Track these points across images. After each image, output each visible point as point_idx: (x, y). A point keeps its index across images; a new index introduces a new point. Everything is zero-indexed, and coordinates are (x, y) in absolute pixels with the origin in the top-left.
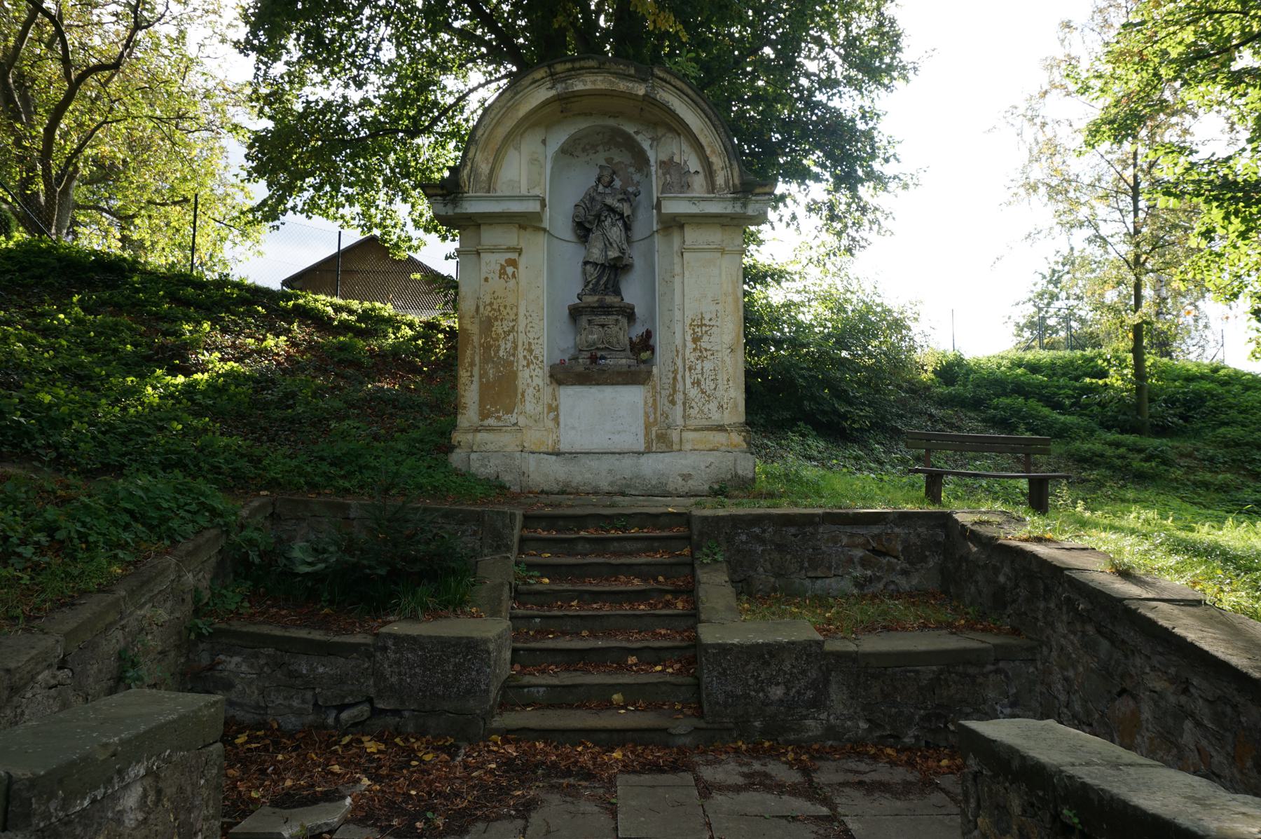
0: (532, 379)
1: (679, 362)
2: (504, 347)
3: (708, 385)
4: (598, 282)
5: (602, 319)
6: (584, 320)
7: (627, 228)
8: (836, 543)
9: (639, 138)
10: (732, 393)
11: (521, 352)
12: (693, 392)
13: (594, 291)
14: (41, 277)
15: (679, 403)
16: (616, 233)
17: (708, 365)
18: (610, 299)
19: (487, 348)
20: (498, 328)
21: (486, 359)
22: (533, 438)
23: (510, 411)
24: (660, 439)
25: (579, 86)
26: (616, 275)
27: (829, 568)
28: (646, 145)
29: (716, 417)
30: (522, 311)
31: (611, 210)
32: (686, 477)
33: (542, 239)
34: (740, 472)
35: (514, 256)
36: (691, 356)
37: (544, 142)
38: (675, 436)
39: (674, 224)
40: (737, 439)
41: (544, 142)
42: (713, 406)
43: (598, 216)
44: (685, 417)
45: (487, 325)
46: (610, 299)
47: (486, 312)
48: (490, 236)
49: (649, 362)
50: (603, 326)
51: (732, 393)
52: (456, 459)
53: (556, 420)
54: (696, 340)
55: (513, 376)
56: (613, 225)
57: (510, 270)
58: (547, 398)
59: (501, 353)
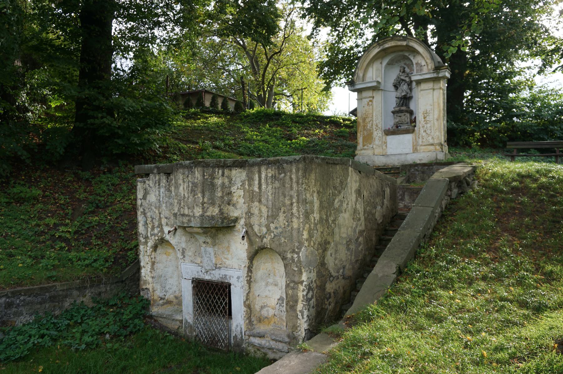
0: (378, 134)
1: (420, 125)
2: (369, 125)
3: (428, 132)
5: (400, 114)
9: (410, 57)
10: (437, 133)
11: (374, 127)
12: (424, 134)
13: (398, 106)
14: (260, 119)
15: (420, 138)
16: (405, 87)
17: (428, 125)
18: (404, 108)
19: (364, 126)
20: (367, 120)
21: (364, 130)
22: (377, 151)
23: (371, 144)
24: (415, 150)
25: (387, 46)
28: (412, 58)
29: (431, 141)
30: (374, 114)
31: (403, 80)
32: (420, 160)
33: (380, 92)
34: (439, 158)
35: (371, 99)
36: (423, 122)
37: (381, 63)
38: (418, 148)
39: (419, 82)
40: (438, 148)
41: (381, 63)
42: (430, 138)
43: (399, 82)
44: (422, 142)
45: (364, 120)
46: (404, 108)
47: (364, 116)
48: (365, 94)
49: (415, 126)
51: (437, 133)
52: (356, 158)
53: (386, 146)
54: (425, 118)
55: (372, 133)
57: (370, 103)
58: (384, 140)
59: (368, 127)
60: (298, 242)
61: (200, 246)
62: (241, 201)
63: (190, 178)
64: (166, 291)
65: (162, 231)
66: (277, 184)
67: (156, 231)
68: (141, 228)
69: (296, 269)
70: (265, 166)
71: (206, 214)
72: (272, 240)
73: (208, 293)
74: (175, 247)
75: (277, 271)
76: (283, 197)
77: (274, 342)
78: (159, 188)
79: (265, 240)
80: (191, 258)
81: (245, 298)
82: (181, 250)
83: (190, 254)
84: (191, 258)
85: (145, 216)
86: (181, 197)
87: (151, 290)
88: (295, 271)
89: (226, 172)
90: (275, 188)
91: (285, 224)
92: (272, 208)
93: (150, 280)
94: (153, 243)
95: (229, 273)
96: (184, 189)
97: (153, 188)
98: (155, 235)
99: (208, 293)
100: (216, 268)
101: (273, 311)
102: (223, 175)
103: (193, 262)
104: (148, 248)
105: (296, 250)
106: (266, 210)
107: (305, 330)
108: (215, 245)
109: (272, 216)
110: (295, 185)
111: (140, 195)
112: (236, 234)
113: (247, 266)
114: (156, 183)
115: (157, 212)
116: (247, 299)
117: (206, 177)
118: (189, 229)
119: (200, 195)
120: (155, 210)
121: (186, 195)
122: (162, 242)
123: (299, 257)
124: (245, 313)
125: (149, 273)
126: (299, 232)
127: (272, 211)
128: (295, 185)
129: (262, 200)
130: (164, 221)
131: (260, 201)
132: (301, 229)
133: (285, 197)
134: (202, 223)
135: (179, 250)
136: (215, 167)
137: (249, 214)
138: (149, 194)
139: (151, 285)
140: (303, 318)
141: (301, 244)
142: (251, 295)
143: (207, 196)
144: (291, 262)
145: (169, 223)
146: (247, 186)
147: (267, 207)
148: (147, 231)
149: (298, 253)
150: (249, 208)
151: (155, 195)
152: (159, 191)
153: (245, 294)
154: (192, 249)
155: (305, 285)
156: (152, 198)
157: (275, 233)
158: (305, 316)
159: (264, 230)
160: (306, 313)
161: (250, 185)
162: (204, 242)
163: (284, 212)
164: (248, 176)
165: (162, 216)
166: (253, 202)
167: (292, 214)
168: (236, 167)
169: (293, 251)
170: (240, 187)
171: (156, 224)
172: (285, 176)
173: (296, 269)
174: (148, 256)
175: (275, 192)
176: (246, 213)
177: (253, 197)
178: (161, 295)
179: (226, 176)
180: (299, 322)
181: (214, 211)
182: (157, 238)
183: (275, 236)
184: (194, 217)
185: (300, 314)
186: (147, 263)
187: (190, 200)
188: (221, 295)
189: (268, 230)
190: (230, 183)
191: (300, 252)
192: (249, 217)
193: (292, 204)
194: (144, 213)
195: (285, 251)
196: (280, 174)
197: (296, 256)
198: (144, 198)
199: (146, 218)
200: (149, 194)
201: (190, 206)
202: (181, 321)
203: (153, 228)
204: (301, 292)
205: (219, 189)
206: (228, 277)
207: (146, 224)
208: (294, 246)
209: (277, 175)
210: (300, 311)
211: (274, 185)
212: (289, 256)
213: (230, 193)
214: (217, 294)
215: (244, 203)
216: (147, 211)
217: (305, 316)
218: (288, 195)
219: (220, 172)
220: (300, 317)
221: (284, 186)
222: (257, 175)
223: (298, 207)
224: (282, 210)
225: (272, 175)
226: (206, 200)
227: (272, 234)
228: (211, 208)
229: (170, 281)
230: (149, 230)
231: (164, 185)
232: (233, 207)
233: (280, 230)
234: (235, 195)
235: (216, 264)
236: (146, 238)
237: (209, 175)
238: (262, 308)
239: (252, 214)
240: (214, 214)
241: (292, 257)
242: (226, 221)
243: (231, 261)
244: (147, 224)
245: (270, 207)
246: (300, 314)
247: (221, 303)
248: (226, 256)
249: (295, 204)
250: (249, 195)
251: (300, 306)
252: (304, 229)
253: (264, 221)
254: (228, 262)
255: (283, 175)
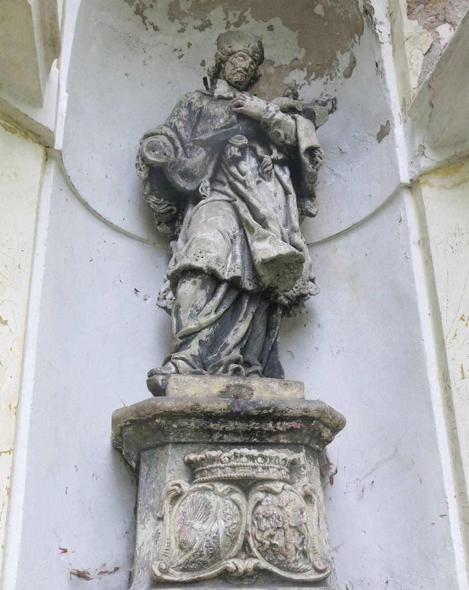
4: (214, 344)
5: (242, 460)
6: (169, 469)
7: (304, 188)
13: (204, 365)
16: (271, 195)
26: (269, 327)
50: (246, 485)
56: (264, 174)
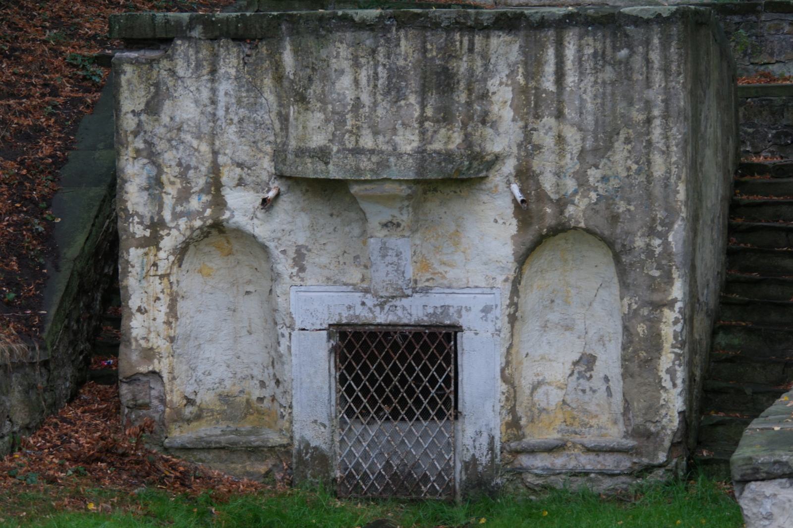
8: (778, 30)
27: (772, 55)
60: (666, 210)
61: (364, 235)
62: (508, 114)
63: (381, 58)
64: (198, 382)
65: (219, 203)
66: (609, 74)
67: (195, 204)
68: (135, 197)
69: (656, 273)
70: (577, 30)
71: (430, 147)
72: (592, 208)
73: (387, 359)
74: (271, 245)
75: (573, 292)
76: (624, 104)
77: (592, 456)
78: (213, 81)
79: (570, 210)
80: (326, 272)
81: (504, 360)
82: (292, 253)
83: (324, 260)
84: (326, 272)
85: (153, 163)
86: (344, 106)
87: (165, 375)
88: (653, 278)
89: (478, 39)
90: (604, 83)
91: (629, 169)
92: (595, 132)
93: (160, 344)
94: (181, 239)
95: (454, 300)
96: (356, 82)
97: (188, 82)
98: (190, 215)
99: (387, 359)
100: (415, 291)
101: (561, 393)
102: (471, 50)
103: (335, 282)
104: (162, 254)
105: (659, 228)
106: (578, 136)
107: (680, 413)
108: (417, 230)
109: (595, 150)
110: (657, 78)
111: (131, 101)
112: (485, 198)
113: (511, 278)
114: (198, 66)
115: (204, 148)
116: (508, 363)
117: (429, 56)
118: (363, 187)
119: (413, 99)
120: (195, 143)
121: (365, 98)
122: (217, 232)
123: (666, 244)
124: (503, 398)
125: (162, 328)
126: (666, 186)
127: (596, 139)
128: (657, 78)
129: (566, 111)
130: (228, 176)
131: (559, 115)
132: (673, 179)
133: (631, 104)
134: (421, 167)
135: (284, 252)
136: (453, 30)
137: (529, 147)
138: (170, 96)
139: (165, 361)
140: (675, 385)
141: (671, 212)
142: (513, 351)
143: (432, 101)
144: (643, 257)
145: (249, 180)
146: (520, 79)
147: (580, 129)
148: (161, 207)
149: (663, 236)
150: (528, 132)
151: (196, 102)
152: (214, 91)
153: (504, 350)
154: (330, 247)
155: (680, 308)
156: (185, 106)
157: (601, 191)
158: (679, 381)
159: (571, 185)
160: (681, 374)
161: (528, 76)
162: (385, 225)
163: (628, 141)
164: (525, 54)
165: (221, 159)
166: (538, 117)
167: (649, 143)
168: (501, 29)
169: (651, 232)
170: (504, 80)
171: (200, 182)
172: (630, 56)
173: (656, 273)
174: (161, 277)
175: (604, 94)
176: (519, 146)
177: (530, 104)
178: (189, 390)
179: (479, 53)
180: (664, 395)
181: (449, 140)
182: (198, 223)
183: (600, 197)
184: (400, 156)
185: (666, 377)
186: (158, 299)
187: (380, 112)
188: (433, 359)
189: (580, 185)
190: (486, 70)
191: (668, 232)
192: (529, 155)
193: (649, 121)
194: (151, 155)
195: (627, 233)
196: (615, 49)
197: (657, 242)
198: (152, 108)
199: (159, 167)
200: (170, 96)
201: (381, 127)
202: (286, 449)
203: (184, 196)
204: (670, 325)
205: (462, 85)
206: (451, 310)
207: (155, 185)
208: (654, 220)
209: (609, 51)
210: (668, 371)
211: (600, 75)
212: (640, 243)
213: (485, 96)
214: (418, 359)
215: (514, 120)
216: (161, 146)
217: (679, 381)
218: (640, 100)
219: (466, 40)
220: (667, 384)
221: (629, 79)
222: (551, 52)
223: (666, 128)
224: (622, 137)
225: (595, 55)
226: (429, 112)
227: (593, 195)
228: (443, 131)
229: (209, 351)
230: (168, 201)
231: (233, 72)
232: (490, 131)
233: (614, 183)
234: (494, 98)
235: (416, 282)
236: (157, 226)
237: (439, 49)
238: (535, 388)
239: (538, 148)
240: (452, 147)
241: (648, 245)
242: (475, 164)
243: (470, 268)
244: (160, 184)
245: (591, 127)
246: (666, 377)
247: (433, 381)
248: (445, 258)
249: (657, 122)
250: (528, 99)
251: (666, 360)
252: (679, 178)
253: (570, 162)
254: (451, 274)
255: (624, 52)
